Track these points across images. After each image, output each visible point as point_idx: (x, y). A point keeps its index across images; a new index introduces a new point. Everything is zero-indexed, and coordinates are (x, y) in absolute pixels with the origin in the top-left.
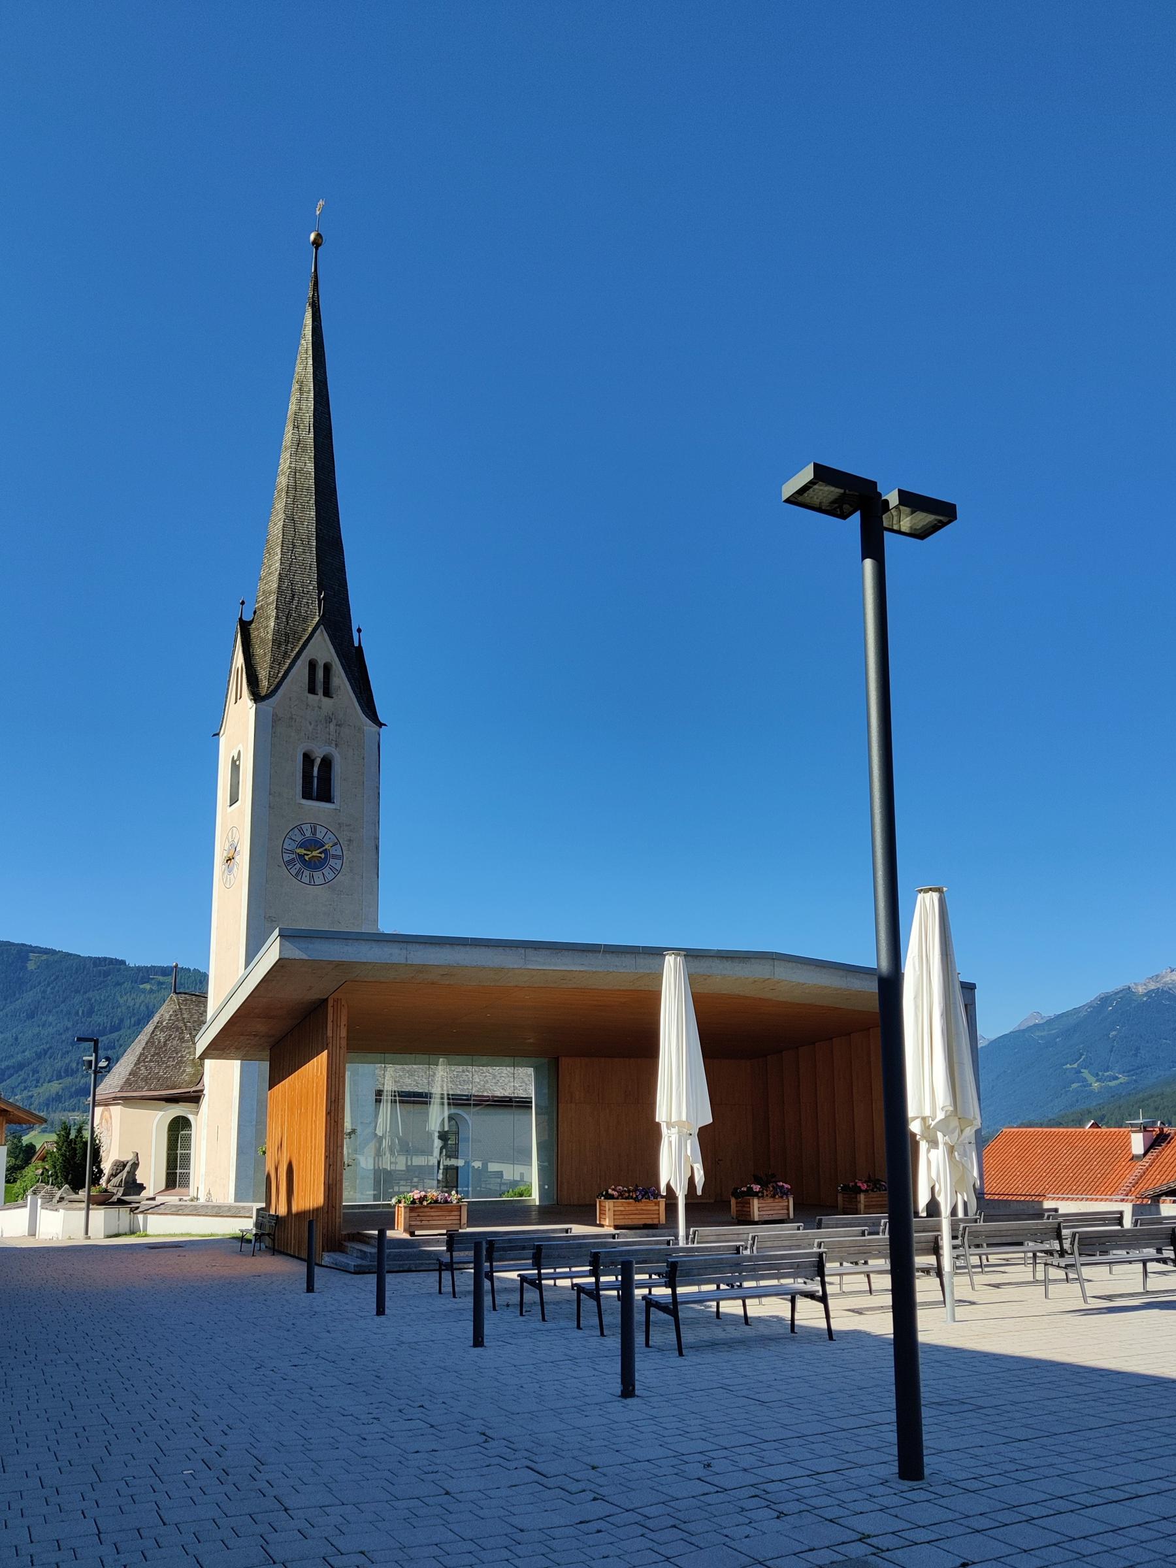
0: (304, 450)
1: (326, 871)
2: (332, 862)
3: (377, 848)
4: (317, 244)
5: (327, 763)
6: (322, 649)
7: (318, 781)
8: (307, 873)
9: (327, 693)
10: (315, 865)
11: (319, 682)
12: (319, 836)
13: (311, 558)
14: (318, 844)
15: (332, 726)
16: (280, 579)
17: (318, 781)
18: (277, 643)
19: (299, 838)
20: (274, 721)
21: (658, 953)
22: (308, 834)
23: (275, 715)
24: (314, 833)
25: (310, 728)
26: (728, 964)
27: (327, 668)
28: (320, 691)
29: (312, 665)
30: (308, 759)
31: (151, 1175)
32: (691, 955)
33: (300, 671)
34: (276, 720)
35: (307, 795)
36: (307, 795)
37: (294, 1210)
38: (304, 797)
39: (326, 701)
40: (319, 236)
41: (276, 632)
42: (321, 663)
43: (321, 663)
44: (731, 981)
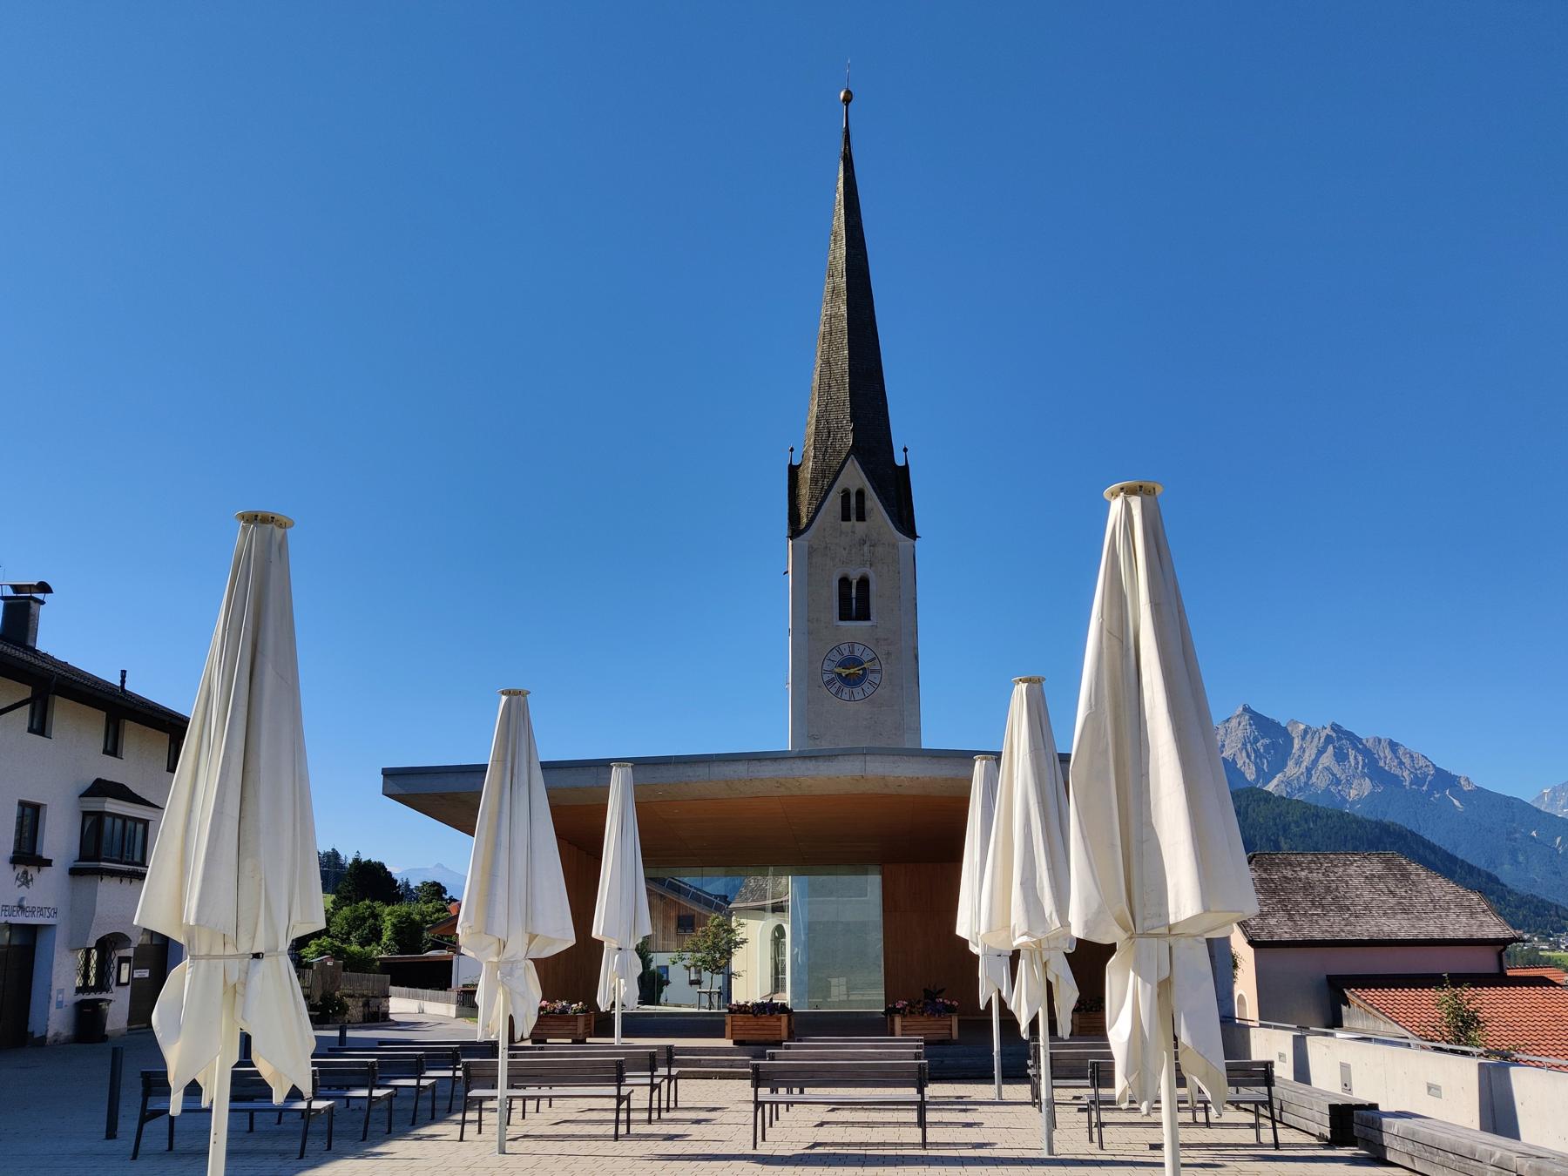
0: (838, 295)
1: (865, 686)
2: (871, 677)
3: (916, 657)
4: (847, 100)
5: (864, 583)
6: (854, 477)
7: (854, 601)
8: (846, 690)
9: (861, 517)
10: (851, 681)
11: (853, 508)
12: (857, 653)
13: (845, 395)
14: (856, 662)
15: (866, 548)
16: (818, 421)
17: (854, 601)
18: (814, 480)
19: (838, 658)
20: (810, 554)
21: (605, 765)
22: (846, 653)
23: (810, 547)
24: (852, 652)
25: (845, 553)
26: (811, 764)
27: (860, 494)
28: (853, 517)
29: (846, 495)
30: (844, 582)
31: (1284, 1071)
32: (638, 763)
33: (834, 501)
34: (812, 551)
35: (845, 615)
36: (845, 615)
37: (1385, 1120)
38: (841, 619)
39: (860, 526)
40: (848, 92)
41: (814, 470)
42: (853, 491)
43: (853, 491)
44: (567, 780)
